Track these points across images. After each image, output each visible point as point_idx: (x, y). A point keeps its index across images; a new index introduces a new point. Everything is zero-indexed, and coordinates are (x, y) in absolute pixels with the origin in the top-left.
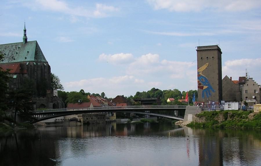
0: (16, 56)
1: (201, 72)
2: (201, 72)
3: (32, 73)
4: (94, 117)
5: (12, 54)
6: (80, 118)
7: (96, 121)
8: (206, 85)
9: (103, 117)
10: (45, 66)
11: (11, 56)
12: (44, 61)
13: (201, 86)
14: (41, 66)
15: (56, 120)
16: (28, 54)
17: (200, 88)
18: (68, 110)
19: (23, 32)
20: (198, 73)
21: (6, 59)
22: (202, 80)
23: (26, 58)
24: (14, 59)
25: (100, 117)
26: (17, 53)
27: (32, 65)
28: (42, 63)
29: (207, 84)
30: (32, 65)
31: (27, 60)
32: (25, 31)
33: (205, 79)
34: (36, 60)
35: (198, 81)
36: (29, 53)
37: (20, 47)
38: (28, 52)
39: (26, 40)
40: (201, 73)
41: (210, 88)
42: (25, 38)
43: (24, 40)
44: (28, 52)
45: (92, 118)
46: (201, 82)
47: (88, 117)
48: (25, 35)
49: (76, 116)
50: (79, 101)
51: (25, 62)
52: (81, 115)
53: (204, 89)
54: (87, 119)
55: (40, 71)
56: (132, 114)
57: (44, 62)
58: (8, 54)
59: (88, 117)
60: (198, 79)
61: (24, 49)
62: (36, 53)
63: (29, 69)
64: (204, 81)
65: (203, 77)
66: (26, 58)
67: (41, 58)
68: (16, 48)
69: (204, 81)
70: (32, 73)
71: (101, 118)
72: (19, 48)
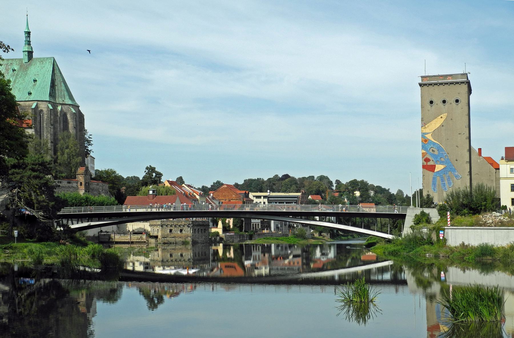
1: (428, 133)
2: (428, 133)
4: (186, 228)
6: (156, 228)
8: (442, 163)
9: (203, 228)
12: (70, 102)
13: (429, 163)
15: (101, 231)
16: (35, 85)
17: (427, 169)
18: (126, 209)
19: (23, 37)
20: (423, 135)
22: (433, 151)
23: (30, 94)
25: (199, 227)
27: (45, 110)
28: (66, 106)
29: (442, 159)
30: (45, 110)
31: (32, 98)
32: (29, 33)
33: (439, 149)
35: (423, 153)
36: (38, 83)
37: (16, 69)
38: (35, 81)
39: (30, 54)
40: (429, 137)
41: (450, 169)
42: (27, 50)
43: (26, 53)
45: (181, 231)
46: (428, 156)
48: (29, 43)
49: (146, 226)
50: (151, 192)
51: (27, 103)
52: (159, 222)
53: (435, 171)
54: (171, 231)
55: (62, 124)
56: (253, 224)
57: (70, 105)
60: (423, 147)
61: (26, 74)
62: (53, 85)
64: (436, 153)
65: (434, 144)
66: (30, 94)
69: (436, 153)
70: (43, 127)
71: (200, 230)
72: (14, 70)
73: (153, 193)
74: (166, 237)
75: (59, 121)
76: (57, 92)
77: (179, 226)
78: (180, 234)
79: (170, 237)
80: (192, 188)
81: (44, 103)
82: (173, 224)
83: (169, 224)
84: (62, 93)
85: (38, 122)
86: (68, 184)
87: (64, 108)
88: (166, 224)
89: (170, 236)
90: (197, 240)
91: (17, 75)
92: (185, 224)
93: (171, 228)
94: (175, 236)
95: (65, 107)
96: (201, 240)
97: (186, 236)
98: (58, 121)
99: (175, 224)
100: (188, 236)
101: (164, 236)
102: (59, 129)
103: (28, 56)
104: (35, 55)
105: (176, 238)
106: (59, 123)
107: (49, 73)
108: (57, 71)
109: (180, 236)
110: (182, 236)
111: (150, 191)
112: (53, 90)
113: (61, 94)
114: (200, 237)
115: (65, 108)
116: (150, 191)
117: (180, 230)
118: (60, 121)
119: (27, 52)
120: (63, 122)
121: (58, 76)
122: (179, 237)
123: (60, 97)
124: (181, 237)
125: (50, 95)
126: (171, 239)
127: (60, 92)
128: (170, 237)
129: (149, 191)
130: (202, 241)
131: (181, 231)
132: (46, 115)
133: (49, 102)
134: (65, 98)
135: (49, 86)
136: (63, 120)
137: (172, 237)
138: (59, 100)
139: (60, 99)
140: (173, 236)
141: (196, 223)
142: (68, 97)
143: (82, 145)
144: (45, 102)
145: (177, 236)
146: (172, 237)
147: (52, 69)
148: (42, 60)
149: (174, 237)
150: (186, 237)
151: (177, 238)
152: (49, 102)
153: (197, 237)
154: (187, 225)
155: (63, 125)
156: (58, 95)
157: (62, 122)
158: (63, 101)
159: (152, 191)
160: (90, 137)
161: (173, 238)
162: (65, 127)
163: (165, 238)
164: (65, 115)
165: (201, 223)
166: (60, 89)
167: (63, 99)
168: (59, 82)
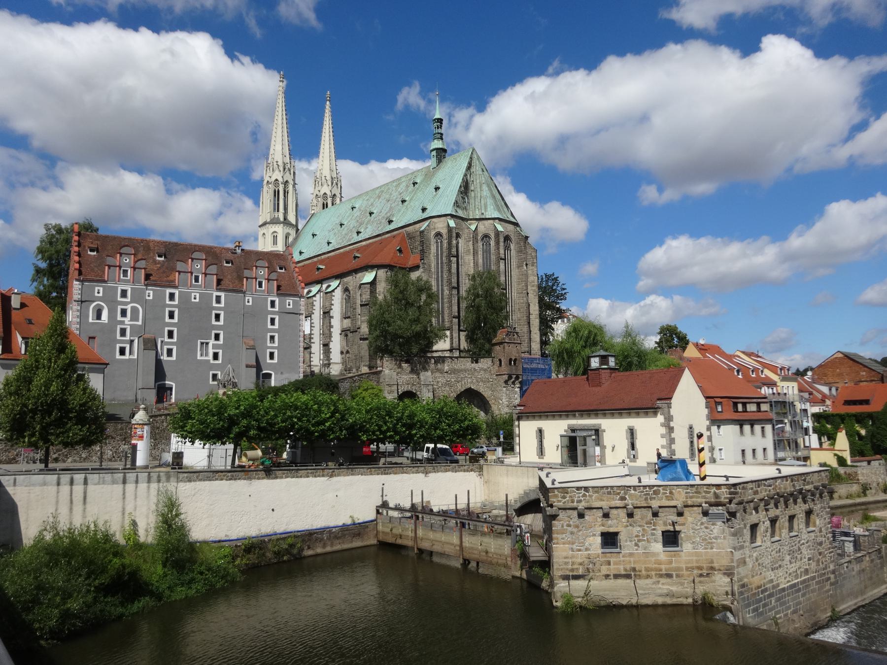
0: (399, 211)
3: (442, 263)
5: (391, 208)
7: (729, 573)
10: (497, 234)
11: (386, 214)
12: (496, 215)
14: (486, 236)
16: (435, 196)
21: (369, 227)
23: (424, 210)
24: (390, 222)
26: (403, 201)
27: (444, 231)
28: (485, 222)
31: (425, 215)
34: (461, 213)
38: (437, 189)
43: (434, 153)
45: (671, 539)
47: (618, 523)
51: (417, 226)
54: (610, 540)
57: (494, 219)
58: (381, 212)
59: (622, 513)
63: (433, 248)
66: (424, 210)
68: (407, 186)
71: (783, 521)
72: (415, 184)
73: (601, 364)
74: (580, 572)
75: (472, 251)
76: (472, 201)
78: (663, 557)
79: (607, 576)
81: (442, 219)
82: (619, 503)
84: (482, 202)
85: (432, 255)
86: (473, 365)
88: (581, 506)
89: (604, 570)
90: (770, 575)
91: (418, 189)
92: (690, 503)
93: (612, 526)
94: (634, 569)
95: (484, 225)
96: (793, 568)
98: (470, 250)
99: (630, 502)
100: (712, 568)
101: (572, 570)
102: (472, 264)
103: (437, 157)
105: (640, 577)
106: (472, 253)
107: (460, 172)
108: (477, 168)
109: (663, 567)
110: (678, 569)
111: (592, 360)
112: (463, 198)
113: (479, 204)
114: (788, 558)
115: (484, 227)
116: (592, 360)
118: (474, 249)
119: (435, 151)
120: (483, 253)
121: (478, 176)
122: (661, 576)
123: (477, 209)
124: (669, 576)
125: (456, 204)
126: (612, 582)
127: (478, 200)
128: (607, 576)
129: (589, 358)
130: (797, 577)
131: (671, 539)
132: (446, 241)
133: (452, 216)
134: (486, 211)
135: (457, 191)
136: (483, 249)
137: (616, 576)
139: (477, 212)
141: (756, 493)
142: (492, 207)
143: (522, 293)
144: (444, 218)
145: (647, 569)
147: (466, 165)
149: (628, 576)
150: (701, 575)
151: (648, 577)
152: (452, 216)
153: (767, 561)
155: (483, 257)
156: (473, 205)
157: (480, 252)
158: (483, 214)
159: (597, 360)
160: (563, 287)
161: (621, 582)
162: (487, 261)
165: (787, 487)
166: (479, 195)
167: (483, 212)
168: (478, 185)
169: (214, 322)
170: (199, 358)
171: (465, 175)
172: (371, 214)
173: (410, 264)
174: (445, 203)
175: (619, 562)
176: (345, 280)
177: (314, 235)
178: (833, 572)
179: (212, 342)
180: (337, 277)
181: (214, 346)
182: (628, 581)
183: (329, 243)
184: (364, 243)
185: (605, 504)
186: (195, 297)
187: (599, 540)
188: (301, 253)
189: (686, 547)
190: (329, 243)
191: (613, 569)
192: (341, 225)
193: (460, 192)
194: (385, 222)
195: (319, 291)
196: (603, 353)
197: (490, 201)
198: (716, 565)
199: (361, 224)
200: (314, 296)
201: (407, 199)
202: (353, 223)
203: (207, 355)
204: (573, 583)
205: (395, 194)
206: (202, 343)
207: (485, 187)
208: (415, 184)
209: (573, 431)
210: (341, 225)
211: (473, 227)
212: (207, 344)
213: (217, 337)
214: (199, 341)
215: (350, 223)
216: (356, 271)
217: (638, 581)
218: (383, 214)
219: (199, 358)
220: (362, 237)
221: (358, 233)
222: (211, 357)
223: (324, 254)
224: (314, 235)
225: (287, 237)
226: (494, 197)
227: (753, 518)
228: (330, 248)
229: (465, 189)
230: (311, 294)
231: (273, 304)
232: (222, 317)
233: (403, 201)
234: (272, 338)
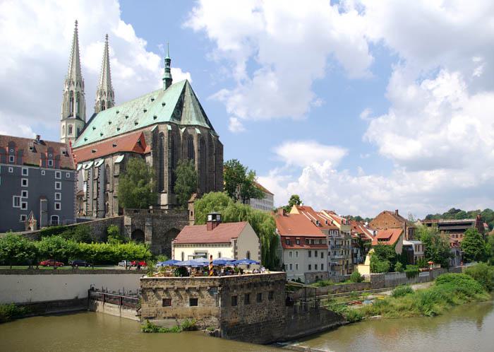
16: (162, 110)
23: (155, 118)
24: (136, 124)
26: (145, 111)
27: (165, 133)
34: (176, 122)
38: (164, 105)
43: (165, 81)
44: (164, 105)
45: (194, 302)
50: (210, 218)
51: (150, 128)
54: (167, 303)
57: (196, 126)
66: (155, 118)
67: (191, 117)
73: (213, 219)
76: (183, 113)
77: (188, 290)
79: (165, 318)
80: (334, 215)
82: (172, 286)
83: (161, 286)
87: (188, 130)
89: (164, 315)
92: (202, 286)
94: (177, 315)
97: (205, 314)
99: (176, 286)
100: (211, 314)
104: (173, 82)
117: (191, 300)
125: (173, 116)
126: (166, 320)
127: (187, 113)
128: (165, 318)
131: (194, 302)
137: (169, 318)
138: (184, 122)
140: (171, 315)
145: (182, 315)
146: (169, 318)
148: (176, 85)
149: (174, 318)
151: (182, 318)
154: (209, 288)
163: (151, 318)
164: (191, 138)
169: (22, 185)
170: (14, 206)
171: (180, 97)
172: (127, 117)
173: (146, 151)
174: (166, 115)
175: (170, 311)
176: (107, 159)
177: (94, 129)
178: (284, 319)
179: (21, 197)
180: (102, 157)
181: (23, 200)
182: (174, 320)
183: (102, 135)
184: (121, 136)
185: (164, 287)
186: (11, 169)
187: (162, 302)
188: (86, 140)
189: (200, 304)
190: (102, 135)
191: (168, 315)
192: (110, 123)
193: (176, 108)
194: (133, 123)
195: (93, 165)
196: (214, 213)
197: (194, 114)
198: (212, 313)
199: (121, 123)
200: (89, 169)
201: (147, 109)
202: (116, 123)
203: (19, 205)
204: (150, 321)
205: (141, 105)
206: (15, 198)
207: (192, 105)
208: (153, 100)
209: (196, 253)
210: (110, 123)
211: (183, 130)
212: (19, 198)
213: (25, 194)
214: (14, 197)
215: (115, 123)
216: (113, 155)
217: (178, 320)
218: (133, 118)
219: (14, 206)
220: (121, 132)
221: (118, 129)
222: (21, 206)
223: (98, 141)
224: (94, 129)
225: (78, 129)
226: (196, 112)
227: (235, 293)
228: (102, 138)
229: (180, 106)
230: (88, 167)
231: (58, 174)
232: (27, 182)
233: (145, 111)
234: (58, 195)
